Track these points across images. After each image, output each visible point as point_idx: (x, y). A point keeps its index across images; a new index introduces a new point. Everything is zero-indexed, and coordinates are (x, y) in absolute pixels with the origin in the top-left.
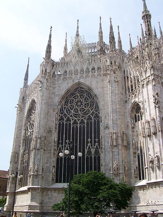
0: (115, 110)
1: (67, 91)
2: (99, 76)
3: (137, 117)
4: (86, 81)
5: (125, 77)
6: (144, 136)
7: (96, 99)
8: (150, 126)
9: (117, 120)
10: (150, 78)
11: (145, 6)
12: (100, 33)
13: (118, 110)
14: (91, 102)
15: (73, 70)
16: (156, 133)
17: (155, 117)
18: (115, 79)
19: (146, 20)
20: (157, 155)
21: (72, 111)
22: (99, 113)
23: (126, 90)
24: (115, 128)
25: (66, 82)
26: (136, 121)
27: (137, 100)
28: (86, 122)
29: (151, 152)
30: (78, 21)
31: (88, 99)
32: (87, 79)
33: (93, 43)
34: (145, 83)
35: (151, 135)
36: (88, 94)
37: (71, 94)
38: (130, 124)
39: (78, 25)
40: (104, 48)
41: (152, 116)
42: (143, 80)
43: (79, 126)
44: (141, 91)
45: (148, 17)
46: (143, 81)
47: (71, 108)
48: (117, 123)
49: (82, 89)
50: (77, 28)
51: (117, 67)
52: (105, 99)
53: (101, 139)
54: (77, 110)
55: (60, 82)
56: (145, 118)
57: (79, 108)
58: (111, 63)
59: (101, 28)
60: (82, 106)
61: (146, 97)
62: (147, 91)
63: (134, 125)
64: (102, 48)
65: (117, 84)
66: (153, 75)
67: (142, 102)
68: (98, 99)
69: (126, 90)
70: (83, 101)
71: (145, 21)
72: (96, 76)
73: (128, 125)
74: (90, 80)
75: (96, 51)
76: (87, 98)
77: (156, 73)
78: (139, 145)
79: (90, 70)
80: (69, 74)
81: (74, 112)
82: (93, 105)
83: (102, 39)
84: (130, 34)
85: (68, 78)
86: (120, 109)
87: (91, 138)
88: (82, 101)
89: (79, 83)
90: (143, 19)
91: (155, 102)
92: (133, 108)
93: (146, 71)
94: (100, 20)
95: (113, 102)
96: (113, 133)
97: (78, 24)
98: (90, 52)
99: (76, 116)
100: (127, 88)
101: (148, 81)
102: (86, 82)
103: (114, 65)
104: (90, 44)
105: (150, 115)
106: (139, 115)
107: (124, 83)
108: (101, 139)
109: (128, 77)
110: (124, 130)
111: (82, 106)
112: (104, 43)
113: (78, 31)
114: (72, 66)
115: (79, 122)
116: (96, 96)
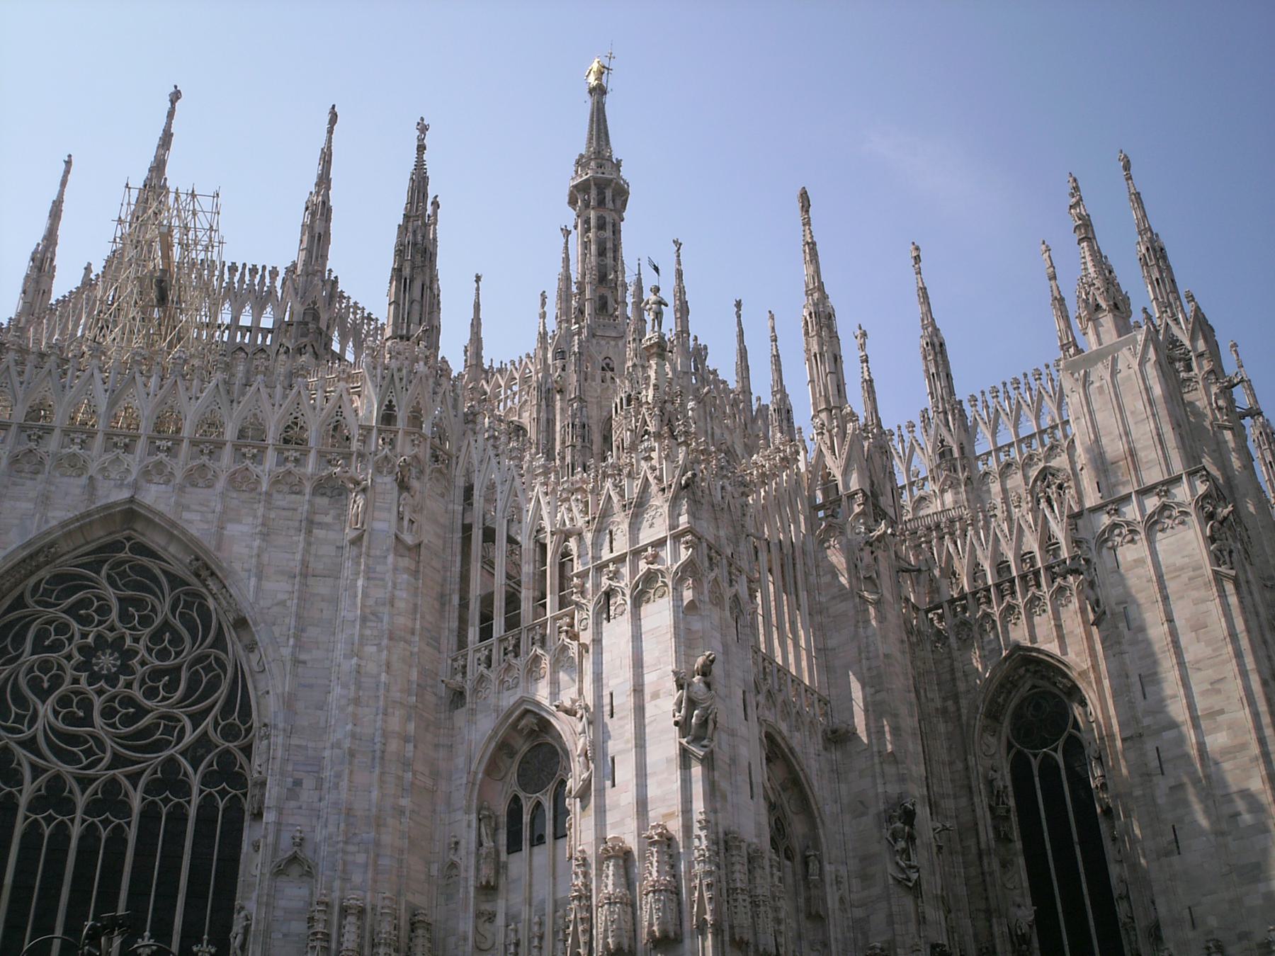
0: (378, 746)
1: (31, 556)
2: (286, 489)
3: (526, 818)
4: (187, 508)
5: (467, 529)
7: (239, 647)
8: (630, 885)
10: (666, 553)
11: (599, 131)
12: (313, 214)
13: (393, 745)
14: (199, 660)
17: (675, 827)
18: (400, 528)
19: (593, 214)
21: (45, 710)
22: (247, 750)
24: (357, 878)
26: (514, 845)
28: (136, 803)
30: (176, 96)
31: (177, 640)
34: (625, 583)
36: (188, 605)
37: (58, 578)
38: (473, 861)
39: (169, 125)
40: (324, 317)
41: (654, 815)
42: (620, 559)
43: (76, 831)
45: (609, 194)
46: (612, 567)
47: (35, 684)
48: (377, 844)
49: (145, 561)
50: (156, 142)
51: (425, 452)
52: (303, 657)
53: (243, 947)
54: (87, 705)
57: (100, 692)
58: (388, 417)
59: (324, 181)
60: (129, 685)
61: (618, 680)
62: (637, 637)
63: (500, 868)
65: (413, 567)
66: (689, 537)
67: (587, 708)
68: (251, 647)
71: (587, 221)
72: (264, 487)
73: (453, 865)
74: (218, 508)
76: (174, 632)
77: (707, 530)
79: (230, 433)
80: (66, 432)
81: (56, 713)
82: (213, 686)
83: (324, 257)
84: (478, 279)
85: (59, 461)
86: (410, 747)
88: (128, 642)
89: (131, 514)
90: (572, 202)
91: (689, 716)
92: (504, 748)
94: (330, 131)
96: (344, 911)
97: (171, 115)
98: (225, 317)
99: (65, 745)
101: (650, 577)
102: (186, 515)
103: (407, 433)
104: (233, 268)
105: (642, 805)
106: (539, 804)
107: (457, 568)
108: (243, 947)
109: (489, 535)
110: (419, 900)
111: (129, 685)
112: (336, 281)
113: (159, 167)
114: (99, 387)
115: (81, 801)
116: (241, 623)
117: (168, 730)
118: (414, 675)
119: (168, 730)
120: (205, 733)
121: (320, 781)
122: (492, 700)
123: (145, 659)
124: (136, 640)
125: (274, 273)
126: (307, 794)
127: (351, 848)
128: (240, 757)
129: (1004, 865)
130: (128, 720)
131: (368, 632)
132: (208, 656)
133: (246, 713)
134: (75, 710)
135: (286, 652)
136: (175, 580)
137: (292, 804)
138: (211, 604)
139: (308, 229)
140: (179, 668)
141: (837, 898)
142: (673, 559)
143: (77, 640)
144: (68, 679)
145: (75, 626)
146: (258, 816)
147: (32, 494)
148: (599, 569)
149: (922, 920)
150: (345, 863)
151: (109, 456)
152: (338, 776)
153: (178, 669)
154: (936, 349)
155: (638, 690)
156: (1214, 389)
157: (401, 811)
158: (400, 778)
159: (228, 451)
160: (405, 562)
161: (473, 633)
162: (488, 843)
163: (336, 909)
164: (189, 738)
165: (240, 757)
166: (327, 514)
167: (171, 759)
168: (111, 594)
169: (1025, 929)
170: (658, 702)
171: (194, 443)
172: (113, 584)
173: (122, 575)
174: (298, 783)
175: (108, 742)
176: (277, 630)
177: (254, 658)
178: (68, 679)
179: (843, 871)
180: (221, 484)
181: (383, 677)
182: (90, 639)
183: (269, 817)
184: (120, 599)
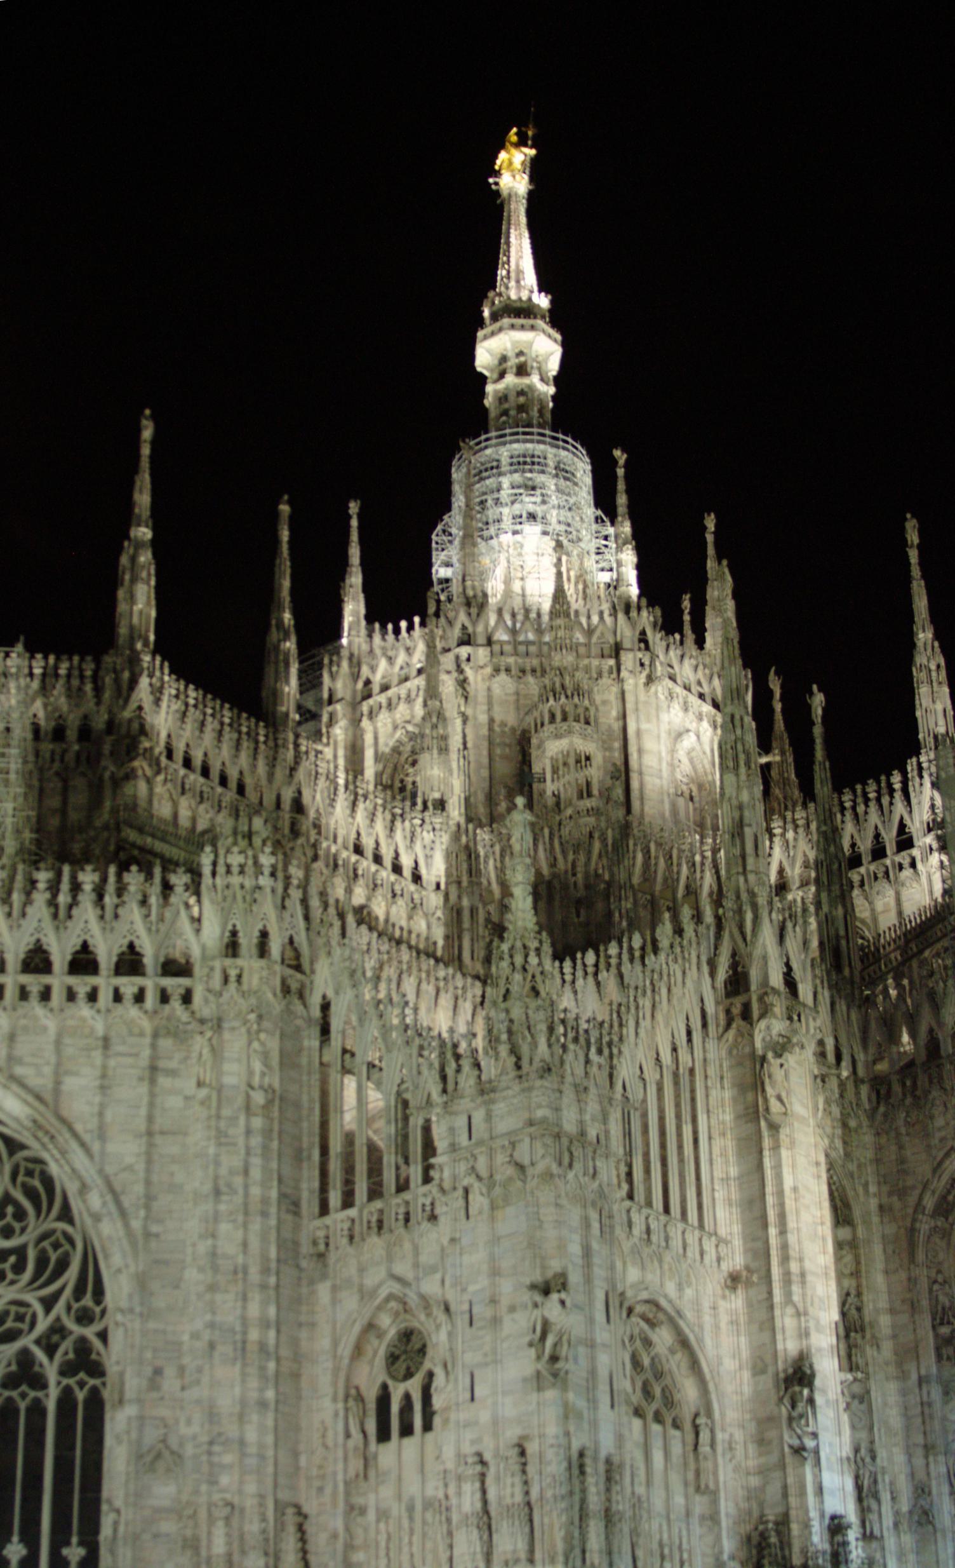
0: (238, 1337)
3: (395, 1408)
4: (20, 1062)
9: (241, 1418)
13: (254, 1335)
22: (103, 1336)
24: (224, 1480)
26: (384, 1435)
48: (242, 1443)
52: (154, 1229)
58: (232, 947)
82: (63, 1265)
86: (272, 1334)
87: (30, 1538)
100: (335, 1167)
118: (273, 1253)
120: (58, 1319)
127: (216, 1448)
128: (97, 1343)
131: (222, 1207)
132: (54, 1231)
133: (99, 1293)
135: (136, 1224)
137: (155, 1395)
138: (54, 1169)
141: (730, 1467)
150: (211, 1464)
155: (493, 1301)
157: (263, 1404)
158: (263, 1369)
161: (335, 1198)
164: (42, 1325)
165: (97, 1343)
166: (170, 1058)
170: (516, 1316)
174: (158, 1372)
176: (126, 1202)
181: (240, 1259)
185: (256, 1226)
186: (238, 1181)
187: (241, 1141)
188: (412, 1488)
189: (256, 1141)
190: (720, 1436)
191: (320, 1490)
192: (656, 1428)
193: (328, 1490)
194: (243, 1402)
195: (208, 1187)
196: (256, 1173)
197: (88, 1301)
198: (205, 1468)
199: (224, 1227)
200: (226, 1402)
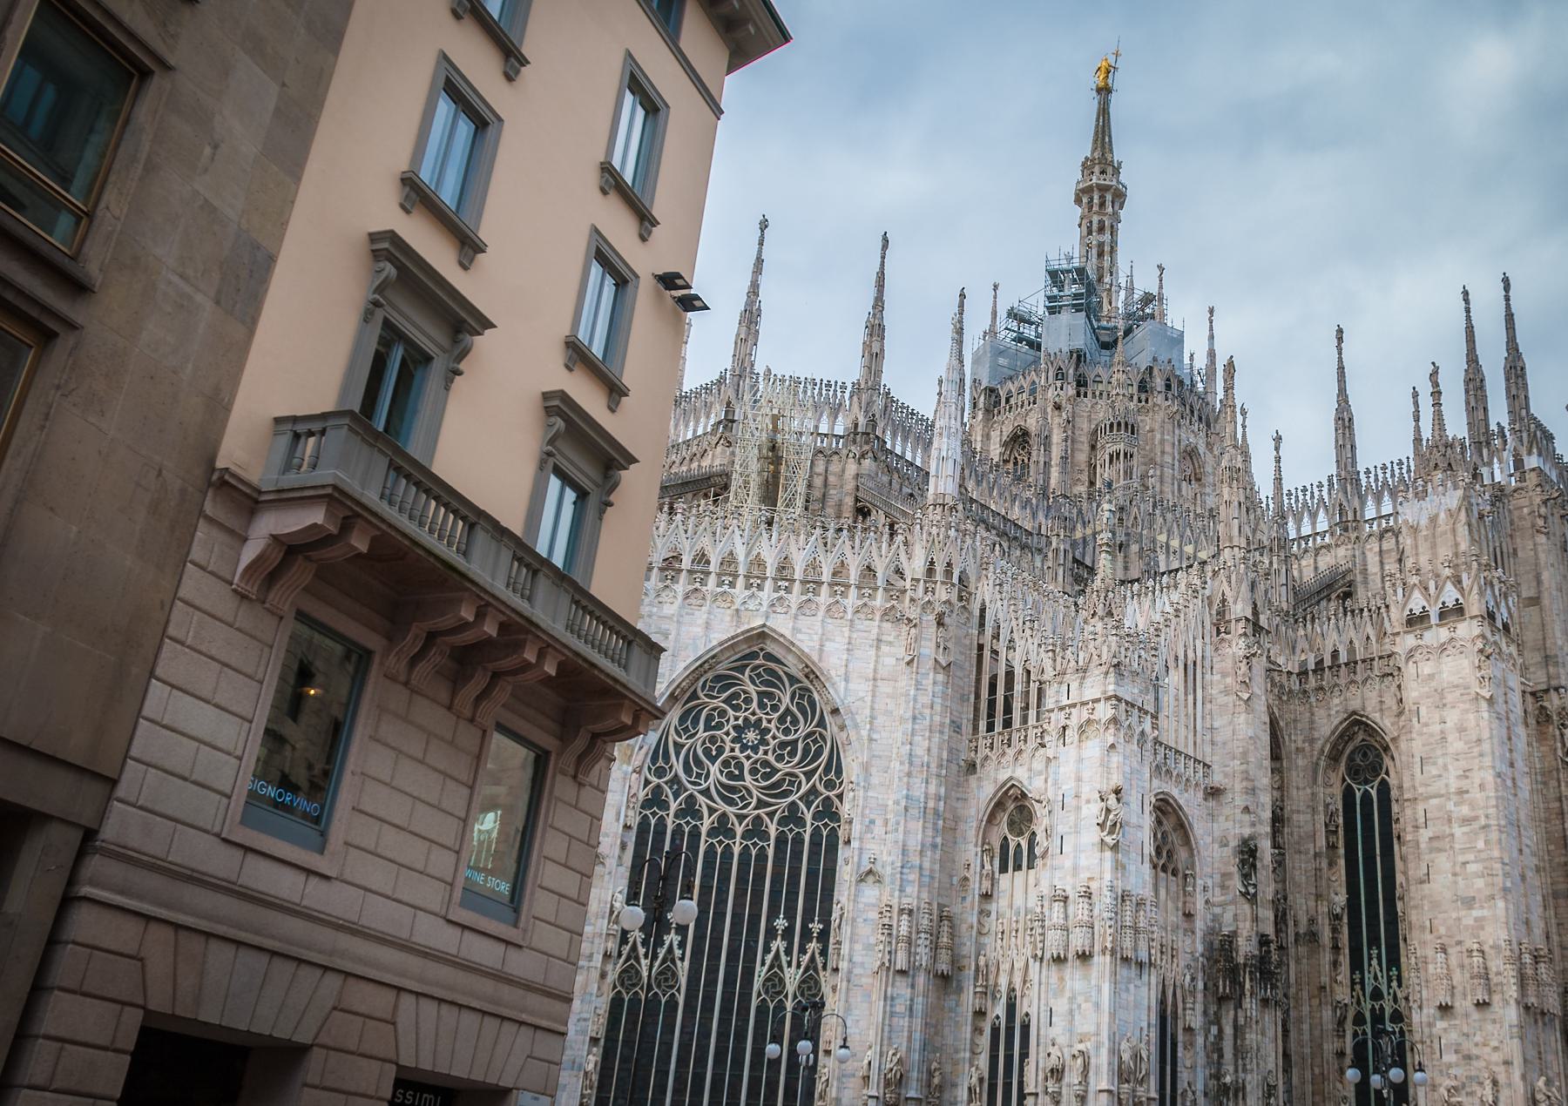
4: (800, 631)
5: (981, 647)
6: (1039, 953)
7: (835, 729)
13: (931, 804)
15: (741, 558)
16: (1091, 956)
20: (1081, 1047)
22: (840, 797)
23: (977, 710)
24: (909, 890)
25: (701, 616)
26: (1003, 869)
27: (1021, 774)
28: (773, 830)
29: (1058, 1031)
31: (795, 722)
32: (803, 622)
33: (829, 385)
35: (1066, 959)
36: (802, 697)
37: (718, 678)
40: (881, 425)
42: (1074, 706)
44: (1050, 752)
48: (921, 868)
49: (772, 665)
51: (954, 599)
52: (875, 736)
54: (740, 766)
55: (668, 610)
56: (1052, 878)
57: (748, 758)
58: (930, 571)
60: (766, 753)
64: (873, 422)
68: (842, 728)
69: (977, 710)
70: (772, 726)
72: (849, 616)
73: (966, 879)
75: (839, 430)
76: (793, 716)
78: (1003, 982)
79: (826, 577)
80: (719, 575)
88: (765, 724)
89: (762, 635)
92: (1000, 805)
93: (1083, 671)
95: (917, 761)
102: (799, 636)
106: (1019, 845)
107: (973, 677)
111: (766, 753)
114: (738, 541)
116: (835, 711)
117: (791, 783)
118: (945, 756)
119: (791, 783)
121: (886, 822)
122: (992, 774)
123: (776, 735)
124: (769, 721)
125: (844, 387)
126: (878, 829)
128: (836, 801)
129: (1331, 864)
130: (766, 776)
133: (839, 772)
134: (733, 769)
135: (864, 733)
136: (793, 680)
138: (816, 696)
139: (867, 346)
140: (796, 741)
142: (1104, 711)
143: (732, 722)
144: (727, 749)
145: (731, 712)
146: (848, 842)
147: (700, 622)
148: (1062, 709)
149: (1256, 919)
151: (747, 593)
152: (898, 823)
153: (796, 741)
154: (1345, 423)
156: (1538, 500)
157: (934, 846)
158: (935, 824)
159: (825, 589)
160: (940, 677)
161: (983, 725)
162: (988, 867)
163: (896, 910)
165: (836, 801)
167: (793, 803)
168: (751, 688)
169: (1339, 910)
171: (804, 582)
172: (754, 683)
173: (759, 675)
174: (872, 822)
175: (755, 792)
177: (844, 735)
178: (727, 749)
179: (1210, 883)
180: (821, 613)
182: (740, 722)
183: (855, 844)
184: (758, 693)
185: (936, 739)
186: (927, 711)
187: (930, 688)
188: (1019, 901)
189: (939, 688)
190: (1199, 882)
191: (964, 898)
192: (1162, 875)
193: (969, 899)
194: (923, 845)
195: (909, 714)
196: (938, 708)
197: (832, 775)
198: (898, 883)
199: (917, 739)
200: (915, 842)
